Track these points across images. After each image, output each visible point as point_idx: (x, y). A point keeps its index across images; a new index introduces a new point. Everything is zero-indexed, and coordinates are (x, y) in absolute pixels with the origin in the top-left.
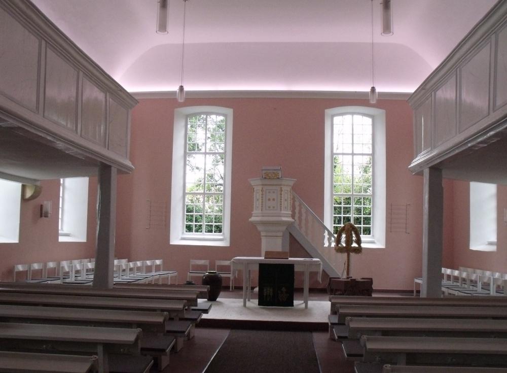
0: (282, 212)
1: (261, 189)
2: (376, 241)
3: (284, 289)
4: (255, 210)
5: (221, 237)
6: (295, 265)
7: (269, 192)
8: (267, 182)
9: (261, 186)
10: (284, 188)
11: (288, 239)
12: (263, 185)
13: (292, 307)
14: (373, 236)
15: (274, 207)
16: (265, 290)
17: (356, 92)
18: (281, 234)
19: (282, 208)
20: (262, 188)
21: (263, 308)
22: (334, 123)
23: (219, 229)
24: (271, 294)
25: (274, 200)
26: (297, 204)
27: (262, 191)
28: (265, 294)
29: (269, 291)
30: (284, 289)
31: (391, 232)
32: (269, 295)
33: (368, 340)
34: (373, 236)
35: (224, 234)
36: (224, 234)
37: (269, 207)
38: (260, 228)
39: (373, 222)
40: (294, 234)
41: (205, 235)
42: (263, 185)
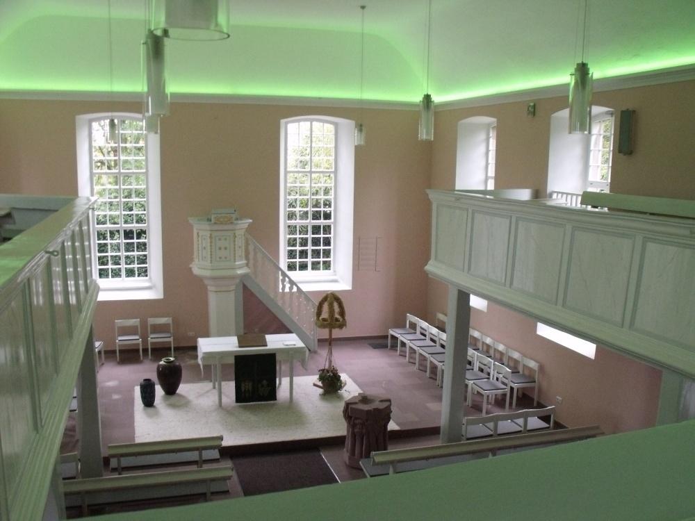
0: (237, 263)
1: (209, 235)
2: (339, 280)
3: (265, 382)
4: (196, 260)
5: (147, 284)
6: (277, 355)
7: (220, 239)
8: (216, 227)
9: (209, 232)
10: (237, 233)
11: (241, 290)
12: (211, 230)
13: (275, 402)
14: (335, 271)
15: (226, 258)
16: (243, 385)
17: (320, 98)
18: (233, 287)
19: (237, 258)
20: (211, 235)
21: (245, 408)
22: (289, 132)
23: (144, 272)
24: (250, 389)
25: (226, 248)
26: (251, 248)
27: (211, 237)
28: (243, 390)
29: (247, 386)
30: (265, 382)
31: (359, 270)
32: (249, 390)
33: (376, 455)
34: (335, 271)
35: (150, 278)
36: (150, 278)
37: (220, 258)
38: (206, 282)
39: (334, 255)
40: (248, 285)
41: (124, 281)
42: (211, 230)
